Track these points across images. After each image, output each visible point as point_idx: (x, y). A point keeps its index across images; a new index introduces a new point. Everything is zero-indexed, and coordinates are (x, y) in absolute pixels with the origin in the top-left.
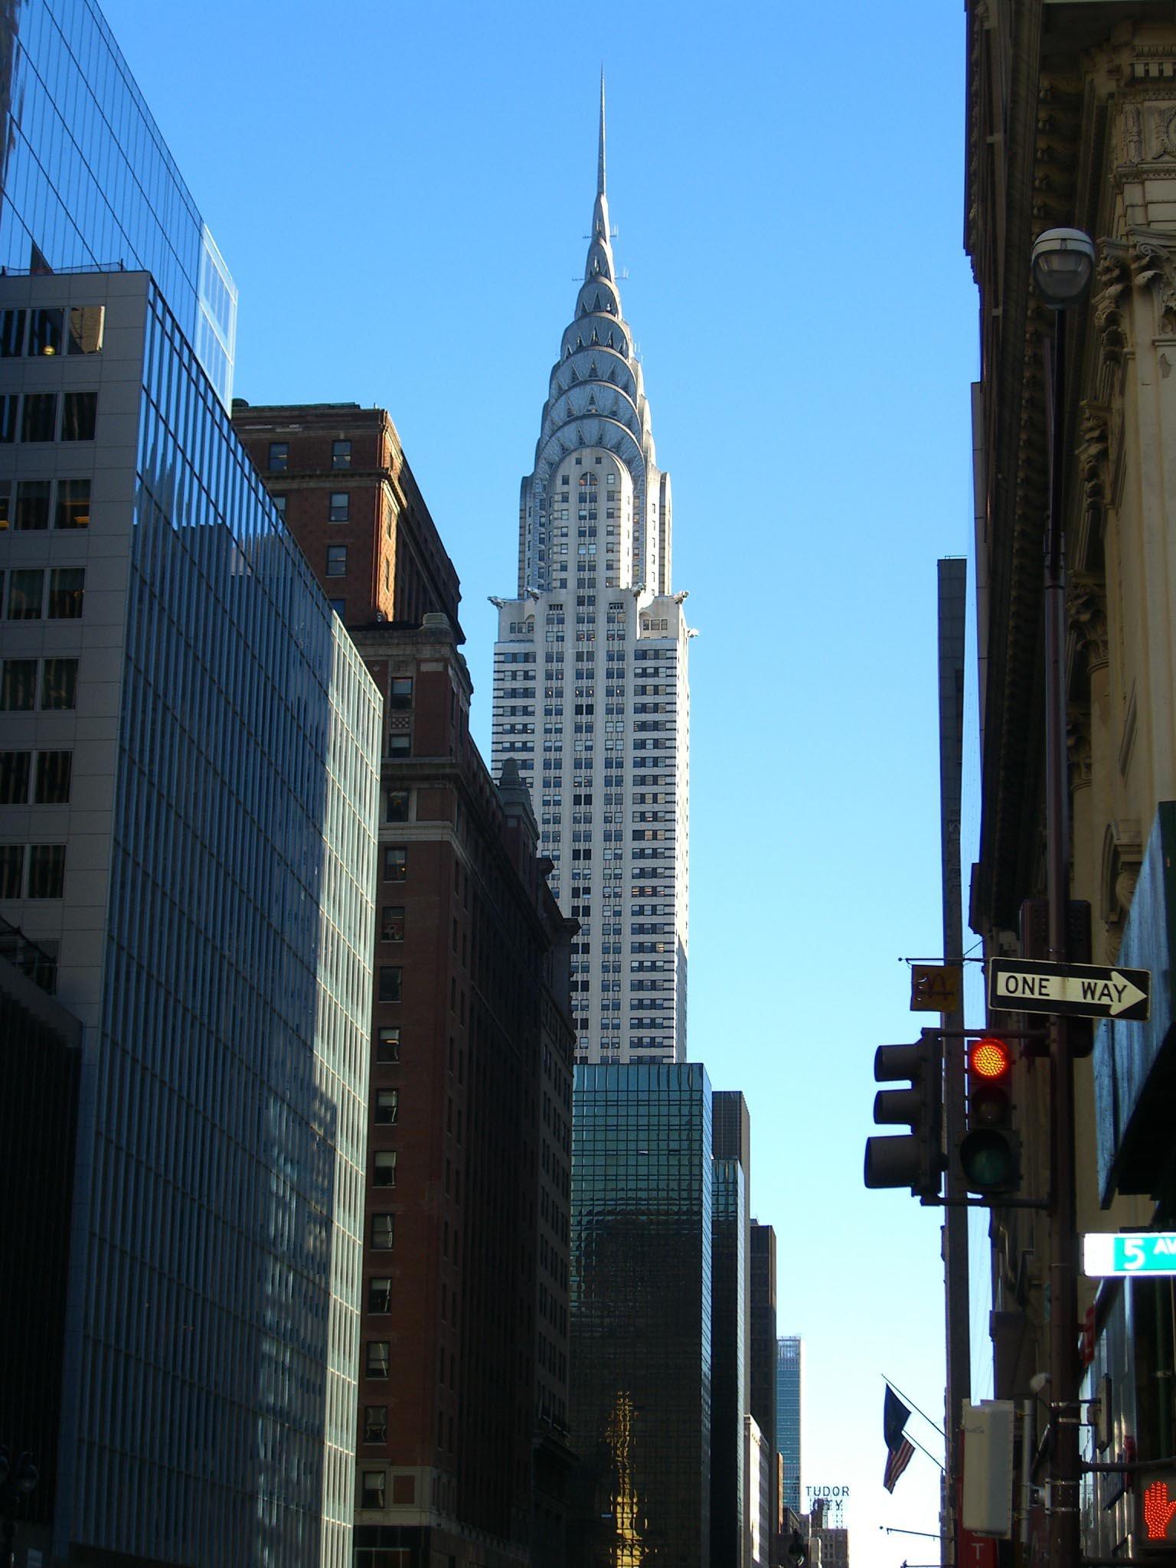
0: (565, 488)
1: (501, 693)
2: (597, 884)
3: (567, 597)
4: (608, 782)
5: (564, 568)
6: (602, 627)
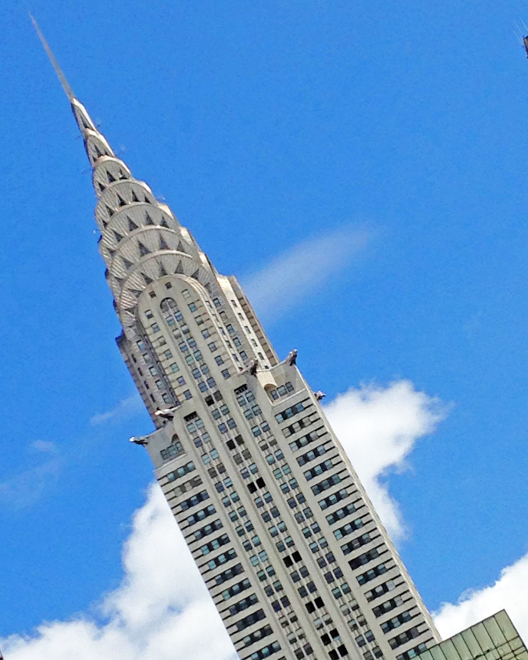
0: (152, 321)
1: (179, 509)
2: (340, 624)
3: (196, 404)
4: (329, 578)
5: (182, 381)
6: (238, 413)
